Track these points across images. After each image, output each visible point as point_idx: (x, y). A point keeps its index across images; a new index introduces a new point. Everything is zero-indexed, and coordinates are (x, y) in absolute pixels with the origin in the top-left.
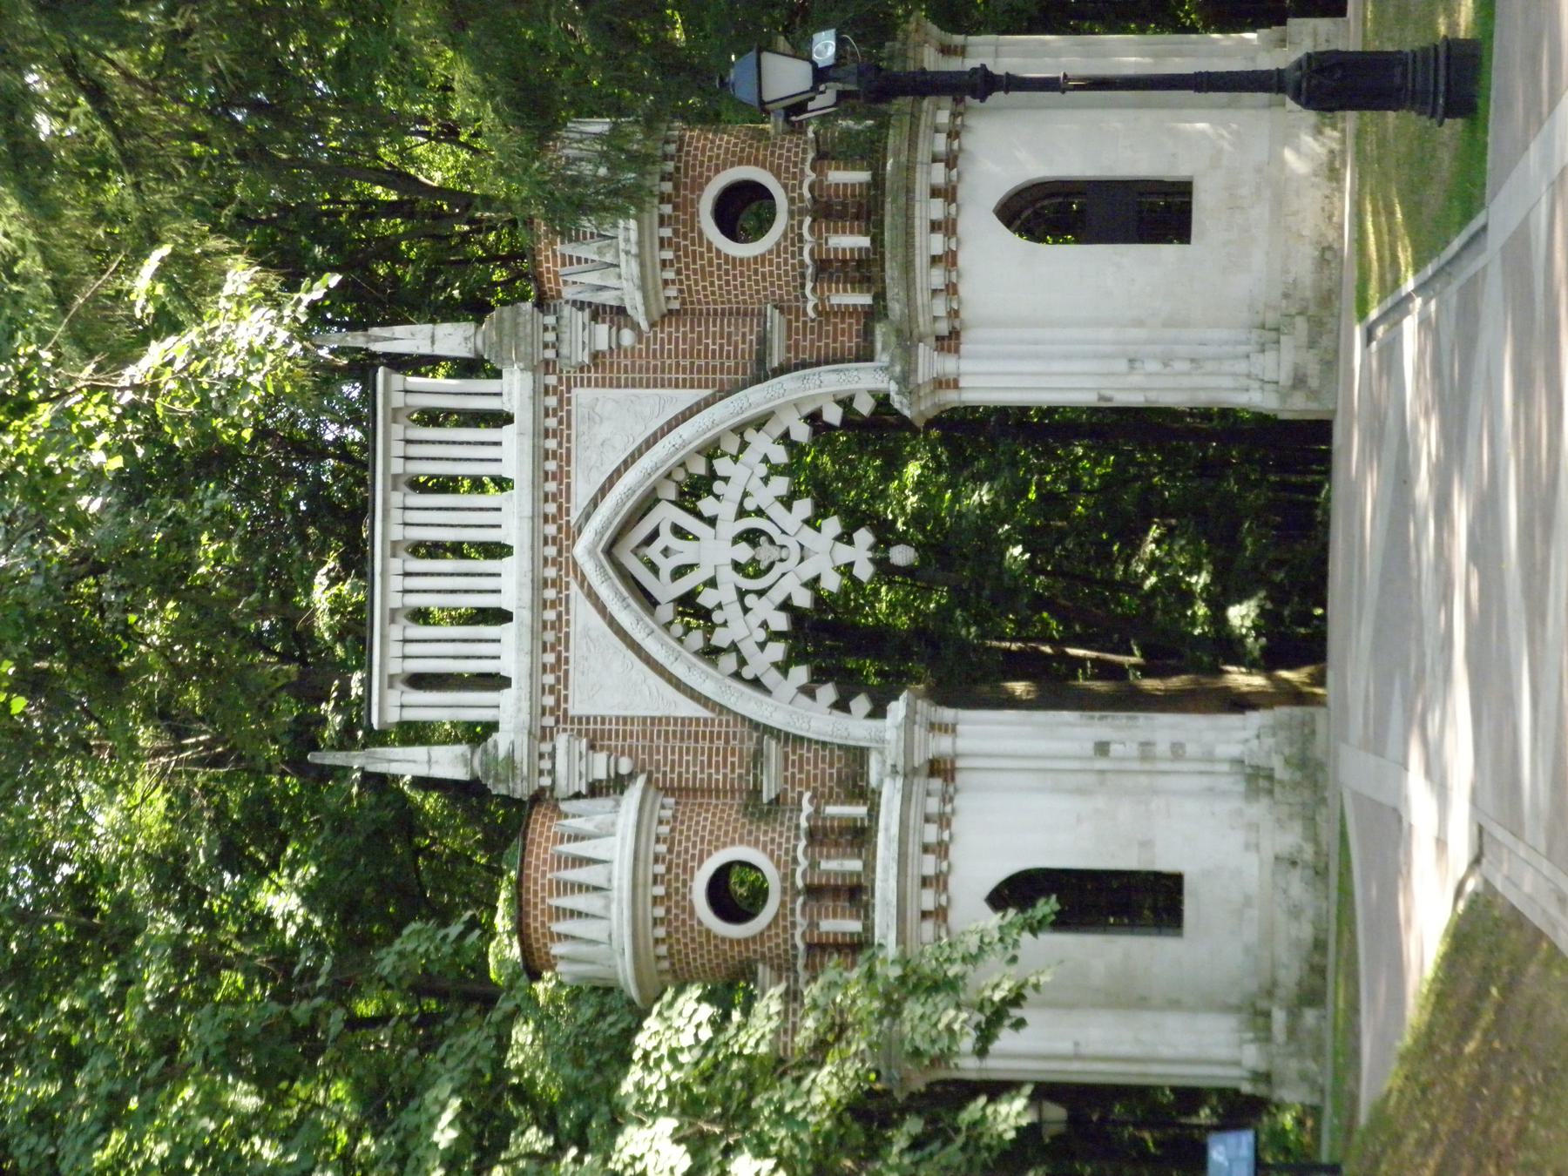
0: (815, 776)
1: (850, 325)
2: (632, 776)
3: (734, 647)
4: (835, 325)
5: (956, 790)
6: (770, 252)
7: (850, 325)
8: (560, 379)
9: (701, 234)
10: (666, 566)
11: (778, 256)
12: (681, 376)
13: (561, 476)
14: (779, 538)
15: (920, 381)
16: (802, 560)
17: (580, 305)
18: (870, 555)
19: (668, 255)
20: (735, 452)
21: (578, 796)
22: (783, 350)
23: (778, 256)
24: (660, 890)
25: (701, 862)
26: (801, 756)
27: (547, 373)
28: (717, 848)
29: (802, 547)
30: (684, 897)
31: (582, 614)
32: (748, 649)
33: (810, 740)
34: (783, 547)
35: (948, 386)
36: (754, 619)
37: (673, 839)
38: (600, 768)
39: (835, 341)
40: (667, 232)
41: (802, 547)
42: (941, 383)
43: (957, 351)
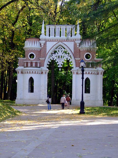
3: (52, 55)
10: (59, 50)
14: (61, 59)
21: (40, 43)
24: (32, 50)
31: (55, 43)
36: (55, 57)
38: (42, 45)
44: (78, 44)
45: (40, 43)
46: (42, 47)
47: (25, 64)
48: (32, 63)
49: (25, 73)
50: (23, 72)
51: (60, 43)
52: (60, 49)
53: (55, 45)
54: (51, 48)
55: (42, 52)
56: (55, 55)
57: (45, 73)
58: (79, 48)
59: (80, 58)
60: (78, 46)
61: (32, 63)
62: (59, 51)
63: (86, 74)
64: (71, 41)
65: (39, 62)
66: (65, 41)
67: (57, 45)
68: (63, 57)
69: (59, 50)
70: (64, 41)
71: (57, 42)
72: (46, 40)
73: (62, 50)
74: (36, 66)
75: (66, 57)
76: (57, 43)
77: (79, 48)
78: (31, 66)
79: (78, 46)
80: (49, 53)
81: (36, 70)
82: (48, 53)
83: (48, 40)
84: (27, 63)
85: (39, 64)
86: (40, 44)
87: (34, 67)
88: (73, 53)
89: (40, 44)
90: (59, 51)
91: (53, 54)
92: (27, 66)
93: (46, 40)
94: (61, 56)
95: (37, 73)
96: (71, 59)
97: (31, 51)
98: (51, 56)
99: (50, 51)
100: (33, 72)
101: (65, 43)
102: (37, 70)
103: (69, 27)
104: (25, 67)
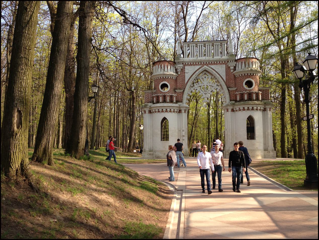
2: (178, 74)
17: (236, 65)
19: (243, 75)
24: (164, 78)
31: (198, 67)
32: (194, 88)
38: (179, 70)
40: (246, 75)
44: (232, 68)
46: (179, 73)
47: (155, 99)
48: (164, 97)
49: (156, 112)
50: (151, 111)
53: (198, 70)
54: (191, 75)
55: (179, 81)
56: (198, 85)
58: (233, 73)
59: (235, 87)
60: (232, 71)
61: (164, 97)
64: (221, 64)
65: (175, 95)
66: (212, 64)
67: (200, 70)
69: (203, 77)
70: (210, 64)
71: (201, 66)
72: (184, 64)
73: (208, 77)
74: (171, 101)
75: (214, 88)
76: (200, 68)
77: (233, 73)
78: (164, 101)
79: (232, 71)
81: (171, 106)
83: (187, 64)
84: (158, 97)
87: (168, 103)
89: (176, 70)
91: (195, 84)
92: (158, 102)
93: (184, 64)
94: (207, 86)
95: (174, 111)
97: (164, 79)
98: (192, 87)
101: (212, 66)
102: (173, 106)
103: (217, 44)
104: (155, 103)
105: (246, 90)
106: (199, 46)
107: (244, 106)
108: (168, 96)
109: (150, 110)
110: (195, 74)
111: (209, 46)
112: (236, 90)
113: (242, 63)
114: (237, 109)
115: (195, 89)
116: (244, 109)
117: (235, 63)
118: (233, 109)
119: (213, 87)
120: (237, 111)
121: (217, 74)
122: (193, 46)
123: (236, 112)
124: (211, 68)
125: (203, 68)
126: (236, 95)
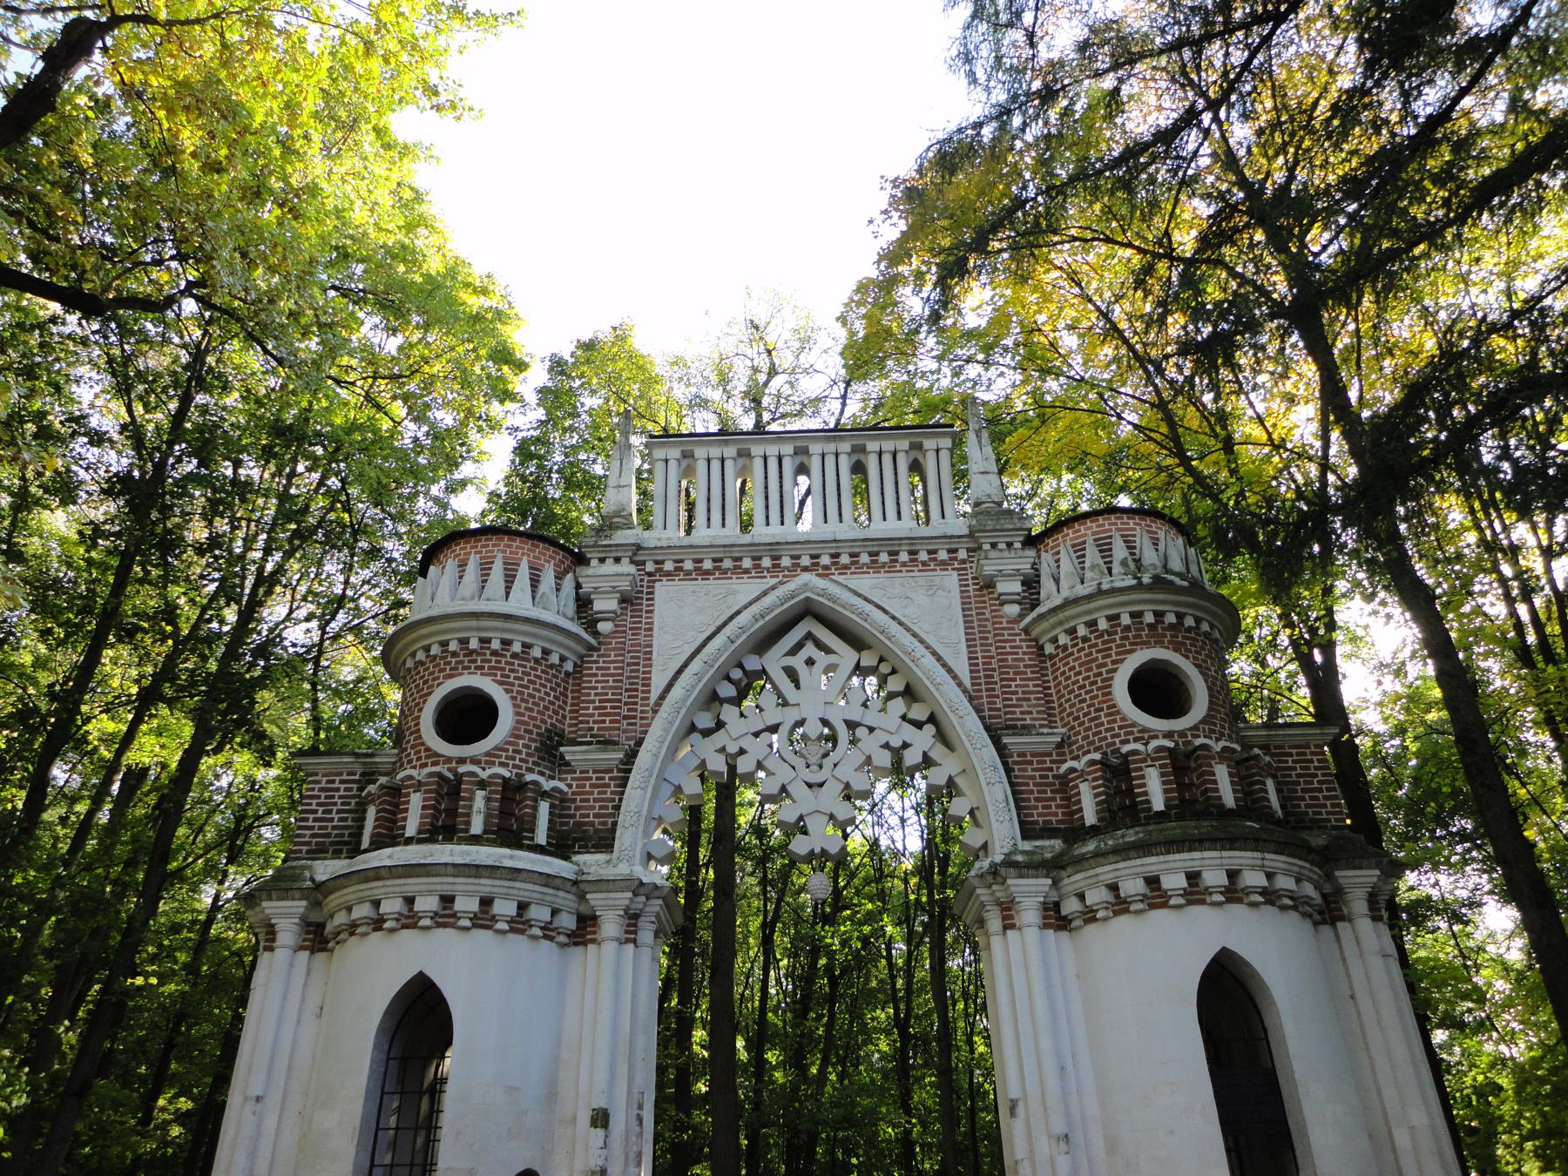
0: (588, 800)
1: (1056, 814)
2: (596, 634)
3: (720, 725)
4: (1054, 799)
5: (562, 945)
6: (1123, 719)
7: (1056, 814)
8: (963, 562)
9: (1131, 651)
10: (797, 661)
11: (1121, 727)
12: (980, 661)
13: (875, 566)
14: (828, 762)
15: (1009, 882)
16: (810, 786)
17: (1035, 567)
18: (817, 850)
19: (1103, 625)
20: (911, 715)
21: (578, 586)
22: (1022, 749)
23: (1121, 727)
24: (474, 644)
25: (500, 683)
26: (608, 786)
27: (968, 550)
28: (514, 698)
29: (821, 785)
30: (465, 668)
32: (720, 738)
33: (622, 793)
34: (821, 767)
35: (1005, 918)
36: (747, 742)
37: (527, 660)
38: (604, 604)
39: (1037, 800)
40: (1126, 620)
41: (821, 785)
42: (1008, 910)
43: (1045, 926)
45: (578, 586)
48: (449, 793)
51: (809, 583)
52: (810, 650)
55: (598, 685)
57: (632, 919)
61: (449, 793)
62: (791, 673)
63: (1195, 910)
68: (843, 734)
69: (797, 661)
73: (832, 659)
74: (510, 831)
75: (881, 737)
78: (445, 826)
79: (1013, 610)
80: (677, 692)
81: (492, 871)
82: (662, 697)
85: (544, 808)
86: (583, 603)
87: (475, 840)
88: (967, 683)
90: (791, 673)
92: (389, 836)
93: (650, 567)
94: (825, 722)
95: (519, 924)
96: (938, 753)
99: (695, 666)
100: (447, 900)
102: (515, 873)
105: (1146, 735)
106: (765, 458)
107: (1152, 864)
108: (482, 784)
109: (315, 917)
110: (727, 631)
111: (830, 461)
112: (1060, 745)
113: (1079, 549)
114: (1096, 896)
115: (733, 749)
116: (1156, 895)
117: (1031, 553)
118: (1057, 905)
119: (871, 729)
120: (1090, 916)
121: (894, 628)
122: (723, 460)
123: (1091, 928)
124: (850, 590)
125: (792, 586)
126: (1065, 786)
